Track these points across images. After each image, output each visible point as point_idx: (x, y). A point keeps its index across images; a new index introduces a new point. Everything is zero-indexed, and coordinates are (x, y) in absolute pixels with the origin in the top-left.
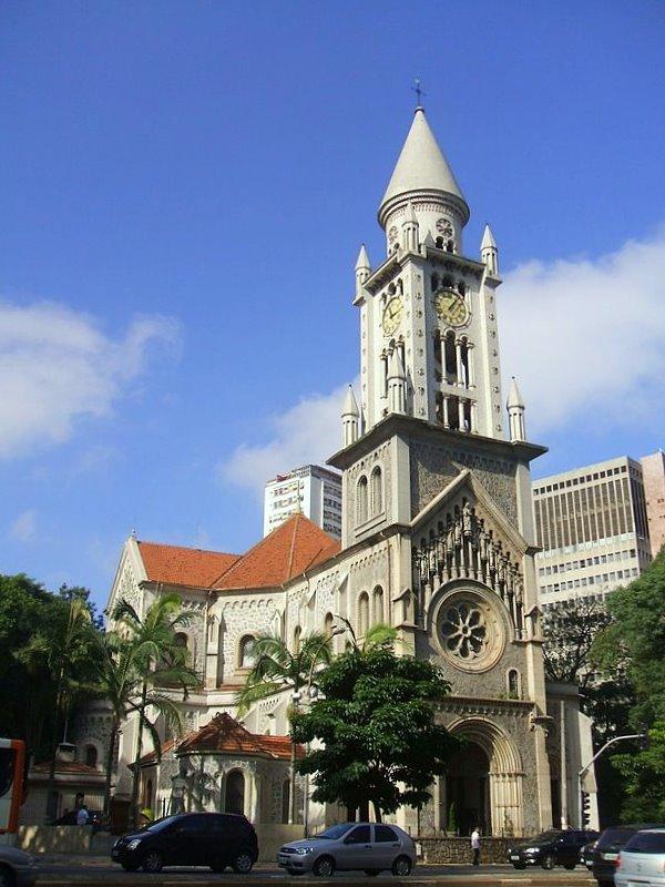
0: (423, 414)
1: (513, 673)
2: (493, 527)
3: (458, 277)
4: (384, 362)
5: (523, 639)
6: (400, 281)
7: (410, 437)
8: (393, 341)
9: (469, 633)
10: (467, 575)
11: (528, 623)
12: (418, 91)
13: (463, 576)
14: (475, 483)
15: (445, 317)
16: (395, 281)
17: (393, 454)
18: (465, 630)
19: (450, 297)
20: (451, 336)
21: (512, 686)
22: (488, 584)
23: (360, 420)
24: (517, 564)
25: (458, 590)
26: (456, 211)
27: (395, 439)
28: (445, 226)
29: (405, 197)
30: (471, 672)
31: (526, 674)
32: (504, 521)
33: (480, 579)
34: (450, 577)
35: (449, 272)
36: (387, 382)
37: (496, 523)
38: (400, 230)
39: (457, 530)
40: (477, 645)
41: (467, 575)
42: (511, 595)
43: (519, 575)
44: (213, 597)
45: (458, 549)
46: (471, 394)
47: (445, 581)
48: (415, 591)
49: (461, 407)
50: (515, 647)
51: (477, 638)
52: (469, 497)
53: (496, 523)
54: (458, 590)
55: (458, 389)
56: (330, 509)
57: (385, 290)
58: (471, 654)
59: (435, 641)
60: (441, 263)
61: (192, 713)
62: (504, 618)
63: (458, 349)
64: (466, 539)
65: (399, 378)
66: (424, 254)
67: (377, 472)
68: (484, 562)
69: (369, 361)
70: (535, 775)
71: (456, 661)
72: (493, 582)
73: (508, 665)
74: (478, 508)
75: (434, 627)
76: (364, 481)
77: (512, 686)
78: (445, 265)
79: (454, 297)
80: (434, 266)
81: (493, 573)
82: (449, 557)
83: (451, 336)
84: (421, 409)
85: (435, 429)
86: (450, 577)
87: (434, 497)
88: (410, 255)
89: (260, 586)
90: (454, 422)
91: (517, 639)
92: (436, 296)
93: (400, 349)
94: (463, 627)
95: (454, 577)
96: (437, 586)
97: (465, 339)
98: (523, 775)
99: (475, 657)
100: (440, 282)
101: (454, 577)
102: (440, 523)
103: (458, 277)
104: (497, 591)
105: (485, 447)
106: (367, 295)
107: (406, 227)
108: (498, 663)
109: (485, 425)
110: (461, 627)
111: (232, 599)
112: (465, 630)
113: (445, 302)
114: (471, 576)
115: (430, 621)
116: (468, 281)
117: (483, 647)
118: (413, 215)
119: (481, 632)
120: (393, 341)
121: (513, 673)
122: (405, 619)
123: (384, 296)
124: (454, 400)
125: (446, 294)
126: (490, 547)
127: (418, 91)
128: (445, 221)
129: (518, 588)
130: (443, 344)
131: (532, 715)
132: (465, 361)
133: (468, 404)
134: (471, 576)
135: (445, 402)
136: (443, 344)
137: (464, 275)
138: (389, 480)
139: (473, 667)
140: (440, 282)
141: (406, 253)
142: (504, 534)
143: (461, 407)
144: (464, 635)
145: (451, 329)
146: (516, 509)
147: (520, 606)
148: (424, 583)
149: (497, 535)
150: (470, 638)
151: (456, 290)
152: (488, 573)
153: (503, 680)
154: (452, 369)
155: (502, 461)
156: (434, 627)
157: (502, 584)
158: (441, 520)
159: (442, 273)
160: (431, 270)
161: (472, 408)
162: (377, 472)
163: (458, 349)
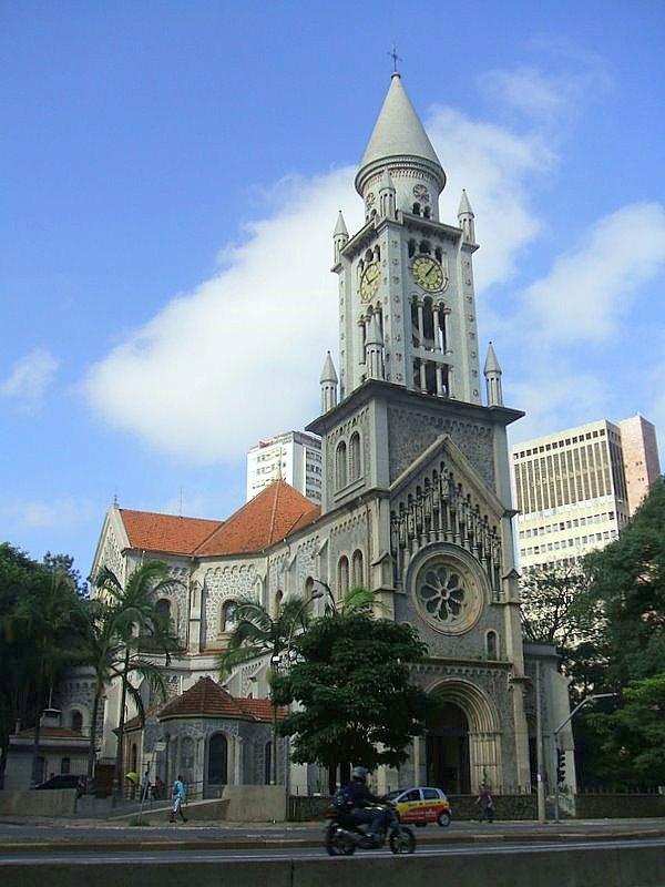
0: (400, 380)
1: (491, 635)
2: (470, 491)
3: (434, 243)
4: (361, 328)
5: (502, 601)
6: (377, 247)
7: (388, 402)
8: (371, 307)
9: (448, 595)
10: (446, 538)
11: (506, 585)
12: (395, 57)
13: (441, 540)
14: (452, 448)
15: (423, 283)
16: (372, 247)
17: (372, 419)
18: (444, 593)
20: (428, 301)
21: (491, 647)
22: (467, 548)
23: (338, 386)
24: (495, 528)
26: (433, 177)
27: (372, 406)
28: (421, 192)
29: (382, 163)
31: (505, 635)
32: (481, 485)
33: (458, 543)
36: (365, 348)
37: (474, 487)
38: (377, 196)
39: (436, 495)
40: (456, 608)
41: (446, 538)
42: (489, 558)
43: (497, 538)
44: (195, 563)
45: (436, 512)
46: (449, 359)
47: (424, 544)
48: (394, 555)
49: (439, 372)
50: (494, 609)
51: (455, 603)
52: (446, 461)
53: (474, 487)
54: (433, 554)
55: (437, 356)
56: (312, 475)
57: (363, 256)
58: (450, 616)
59: (415, 602)
61: (175, 677)
62: (481, 580)
63: (436, 314)
64: (444, 503)
65: (377, 344)
66: (401, 220)
67: (356, 437)
68: (462, 526)
69: (347, 328)
70: (514, 733)
71: (434, 623)
72: (471, 546)
73: (487, 627)
74: (456, 474)
75: (413, 590)
76: (342, 446)
77: (491, 647)
78: (422, 231)
79: (431, 263)
80: (411, 232)
81: (471, 536)
82: (428, 521)
83: (428, 301)
84: (400, 374)
85: (413, 394)
87: (412, 461)
88: (386, 221)
89: (241, 551)
90: (432, 387)
92: (414, 262)
93: (377, 316)
94: (442, 591)
96: (416, 549)
97: (442, 305)
98: (501, 734)
99: (454, 619)
100: (417, 248)
101: (433, 541)
102: (418, 488)
103: (434, 243)
104: (475, 555)
105: (463, 411)
106: (345, 261)
107: (382, 193)
108: (476, 624)
109: (461, 390)
110: (439, 591)
111: (214, 565)
112: (444, 593)
113: (423, 267)
114: (450, 540)
115: (409, 583)
116: (445, 247)
117: (462, 610)
118: (390, 181)
119: (459, 594)
120: (371, 307)
121: (491, 635)
122: (384, 583)
124: (431, 366)
125: (423, 260)
126: (468, 512)
127: (395, 57)
128: (422, 186)
130: (420, 310)
131: (510, 676)
132: (443, 329)
133: (446, 369)
134: (450, 540)
136: (420, 310)
137: (442, 240)
138: (367, 446)
139: (452, 629)
140: (417, 248)
141: (384, 219)
142: (482, 498)
143: (439, 372)
145: (428, 295)
146: (494, 473)
147: (497, 568)
148: (402, 547)
149: (475, 499)
150: (449, 600)
151: (433, 256)
154: (429, 334)
155: (479, 425)
156: (413, 590)
157: (480, 547)
159: (419, 238)
160: (408, 236)
161: (450, 374)
162: (356, 437)
163: (436, 314)
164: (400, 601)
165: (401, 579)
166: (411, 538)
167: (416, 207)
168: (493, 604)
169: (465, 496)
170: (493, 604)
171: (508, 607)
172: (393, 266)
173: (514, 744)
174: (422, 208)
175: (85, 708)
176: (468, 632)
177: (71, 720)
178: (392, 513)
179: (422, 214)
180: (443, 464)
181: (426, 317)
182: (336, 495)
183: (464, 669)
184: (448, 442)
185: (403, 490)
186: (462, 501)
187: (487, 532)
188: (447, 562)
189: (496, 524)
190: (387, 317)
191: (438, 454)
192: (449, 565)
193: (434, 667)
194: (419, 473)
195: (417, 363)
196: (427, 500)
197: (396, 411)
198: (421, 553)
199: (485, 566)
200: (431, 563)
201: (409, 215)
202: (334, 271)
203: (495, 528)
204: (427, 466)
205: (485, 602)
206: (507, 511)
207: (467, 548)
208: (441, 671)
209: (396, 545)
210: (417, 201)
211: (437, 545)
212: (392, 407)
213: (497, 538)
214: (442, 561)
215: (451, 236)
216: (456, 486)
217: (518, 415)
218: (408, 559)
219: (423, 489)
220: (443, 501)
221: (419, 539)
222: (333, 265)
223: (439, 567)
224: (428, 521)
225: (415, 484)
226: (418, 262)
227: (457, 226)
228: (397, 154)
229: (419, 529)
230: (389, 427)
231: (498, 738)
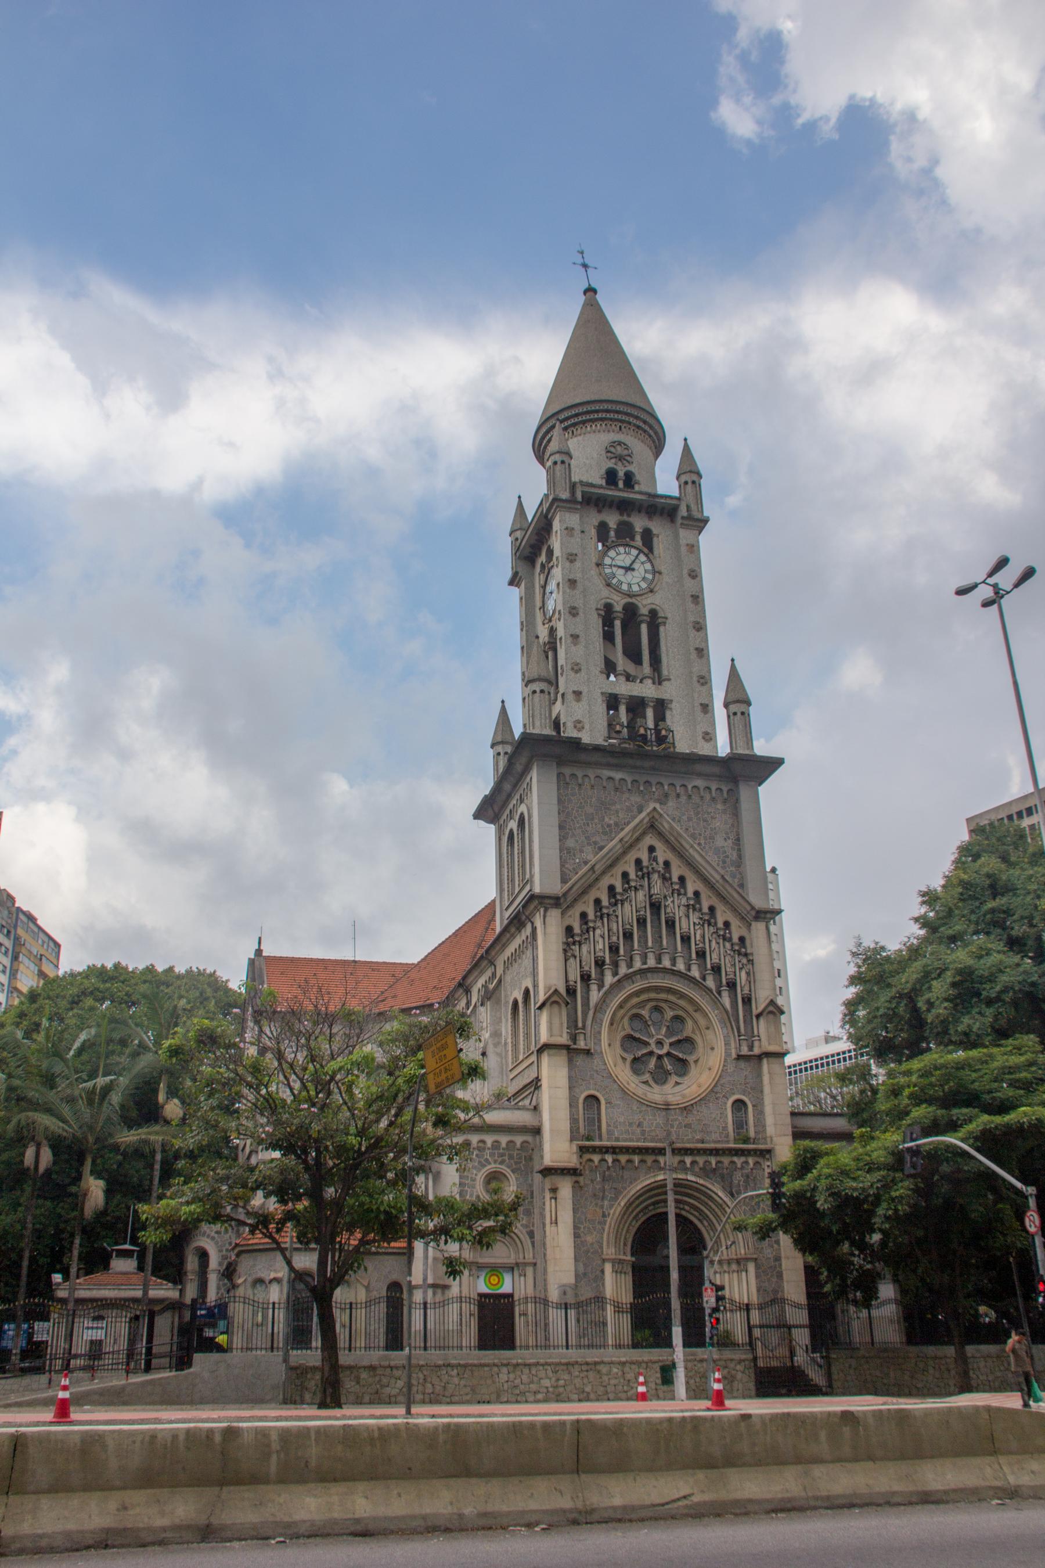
1: (739, 1105)
2: (700, 887)
3: (639, 523)
5: (756, 1051)
9: (664, 1051)
10: (659, 960)
13: (651, 962)
19: (629, 554)
21: (740, 1124)
24: (742, 939)
25: (639, 984)
26: (638, 427)
27: (534, 774)
30: (667, 1107)
31: (763, 1104)
33: (681, 966)
34: (630, 965)
35: (625, 518)
37: (705, 881)
39: (641, 895)
41: (659, 960)
42: (732, 985)
43: (746, 955)
46: (668, 691)
47: (623, 970)
48: (571, 991)
49: (650, 713)
50: (742, 1064)
53: (705, 881)
54: (639, 984)
55: (647, 690)
60: (611, 506)
63: (644, 628)
64: (656, 907)
66: (579, 496)
70: (778, 1259)
72: (702, 967)
79: (634, 552)
80: (599, 511)
82: (628, 936)
86: (630, 965)
87: (601, 848)
88: (555, 500)
91: (745, 1051)
92: (605, 553)
95: (638, 964)
96: (609, 979)
99: (677, 1083)
100: (612, 534)
101: (638, 964)
102: (611, 889)
110: (652, 1041)
112: (660, 1043)
114: (666, 963)
116: (657, 527)
123: (543, 566)
124: (637, 706)
125: (621, 549)
126: (694, 917)
129: (743, 974)
130: (618, 623)
133: (661, 707)
135: (623, 709)
136: (618, 623)
139: (671, 1099)
140: (612, 534)
143: (650, 713)
144: (653, 1047)
145: (630, 600)
147: (747, 1001)
151: (638, 541)
152: (694, 956)
153: (723, 1115)
158: (612, 882)
159: (612, 520)
160: (594, 518)
163: (644, 628)
164: (580, 1060)
165: (584, 1027)
166: (600, 963)
167: (611, 477)
168: (739, 1057)
169: (690, 894)
170: (739, 1057)
171: (765, 1061)
172: (568, 564)
173: (780, 1275)
174: (621, 474)
175: (212, 1243)
176: (703, 1100)
177: (196, 1259)
178: (569, 930)
179: (621, 484)
180: (652, 849)
181: (632, 632)
182: (507, 909)
183: (688, 1160)
184: (657, 816)
185: (584, 892)
186: (684, 901)
187: (728, 945)
188: (663, 996)
189: (744, 932)
190: (561, 639)
191: (644, 834)
192: (666, 1001)
193: (636, 1159)
194: (611, 866)
195: (612, 702)
196: (626, 905)
197: (573, 775)
198: (618, 985)
199: (726, 1000)
200: (635, 1000)
201: (600, 487)
202: (511, 583)
203: (742, 939)
204: (624, 853)
205: (728, 1054)
206: (758, 912)
207: (695, 973)
208: (649, 1163)
209: (574, 975)
210: (611, 464)
211: (642, 972)
212: (567, 771)
213: (746, 955)
214: (653, 995)
215: (665, 510)
216: (675, 879)
217: (773, 764)
218: (595, 995)
219: (619, 889)
220: (652, 905)
221: (615, 965)
222: (509, 574)
223: (654, 1004)
224: (628, 936)
225: (606, 882)
226: (612, 553)
227: (676, 494)
228: (578, 401)
229: (614, 949)
230: (560, 801)
231: (751, 1267)
